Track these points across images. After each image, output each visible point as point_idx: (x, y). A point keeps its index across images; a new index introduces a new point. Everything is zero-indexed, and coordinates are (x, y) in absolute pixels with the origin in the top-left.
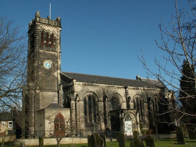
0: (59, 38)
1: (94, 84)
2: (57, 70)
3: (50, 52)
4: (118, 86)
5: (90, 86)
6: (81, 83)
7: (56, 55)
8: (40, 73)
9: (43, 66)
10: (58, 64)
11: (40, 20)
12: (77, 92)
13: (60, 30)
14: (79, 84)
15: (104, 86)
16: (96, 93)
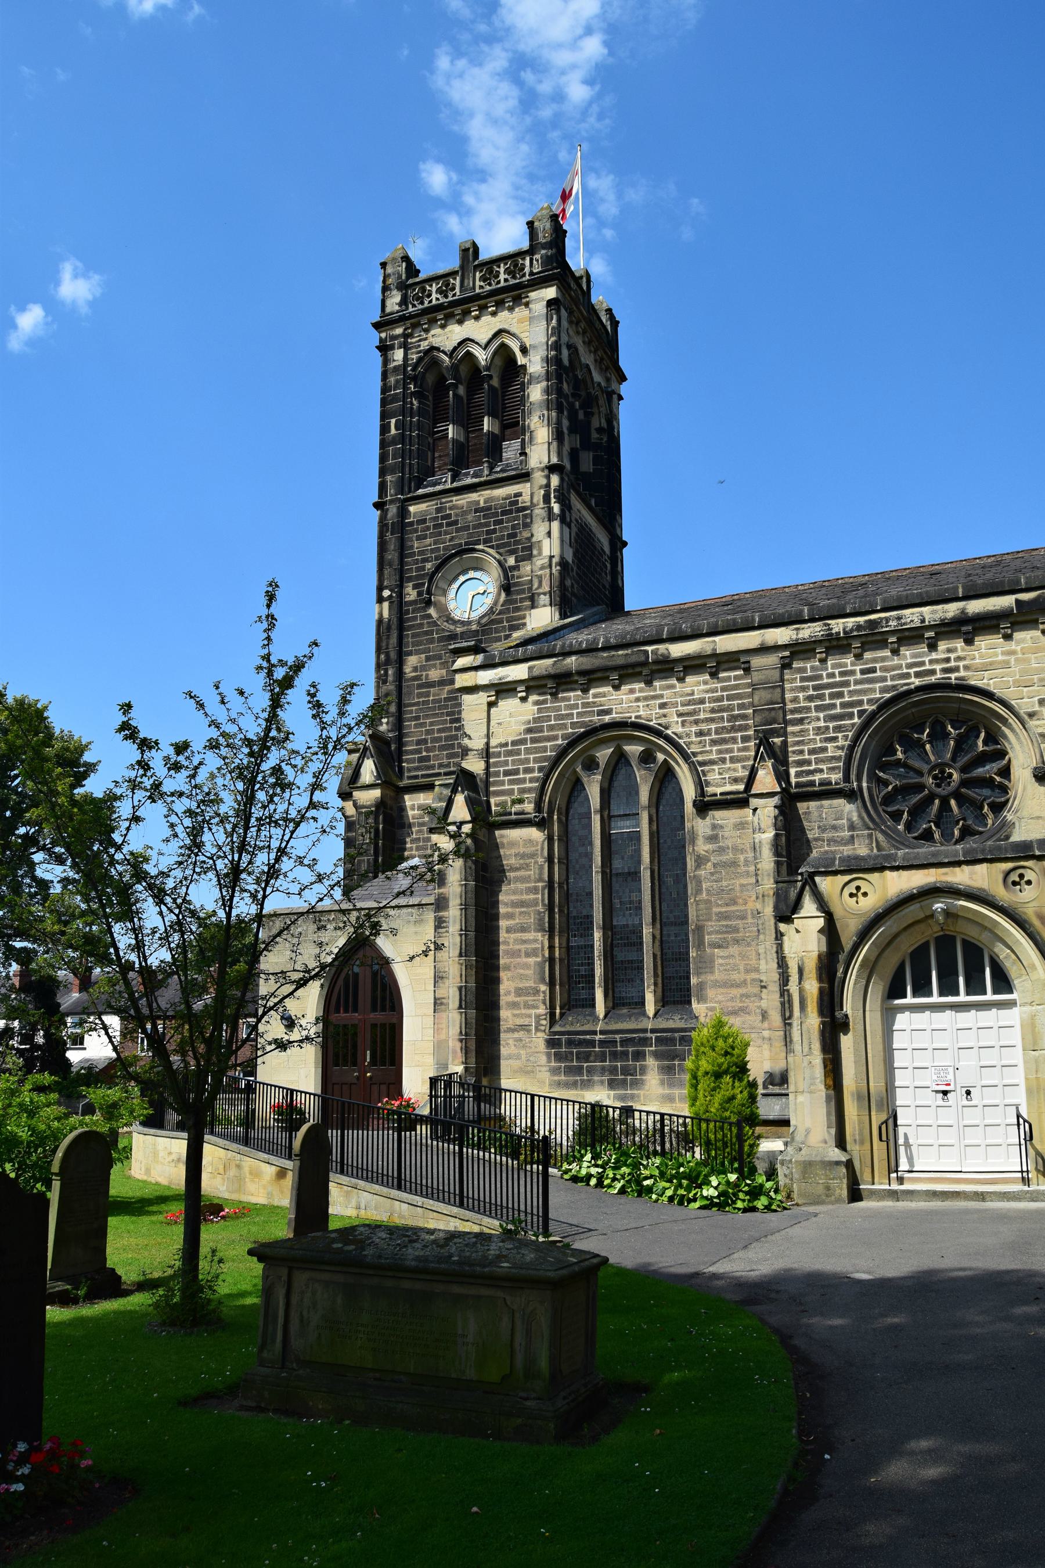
0: (547, 360)
1: (650, 648)
2: (533, 607)
3: (480, 497)
4: (951, 610)
5: (614, 676)
6: (518, 672)
7: (526, 498)
8: (412, 661)
9: (432, 611)
10: (540, 562)
11: (404, 302)
12: (487, 753)
13: (550, 303)
14: (503, 690)
15: (764, 649)
16: (675, 728)
